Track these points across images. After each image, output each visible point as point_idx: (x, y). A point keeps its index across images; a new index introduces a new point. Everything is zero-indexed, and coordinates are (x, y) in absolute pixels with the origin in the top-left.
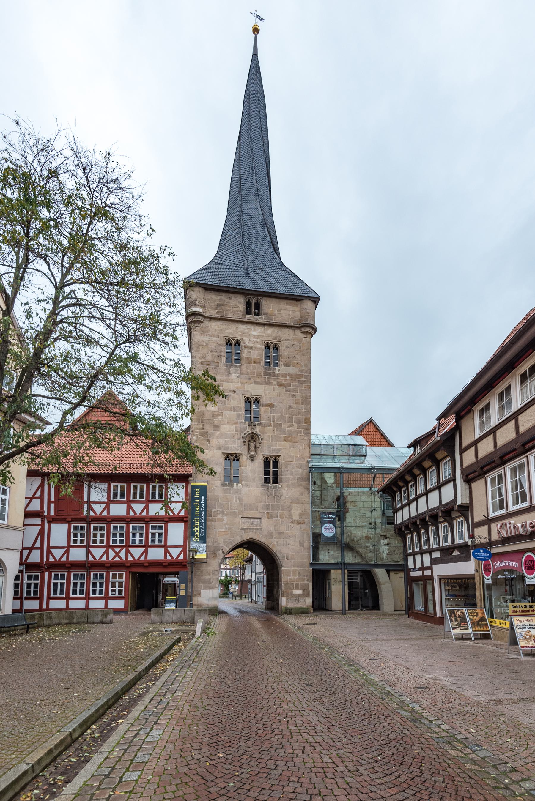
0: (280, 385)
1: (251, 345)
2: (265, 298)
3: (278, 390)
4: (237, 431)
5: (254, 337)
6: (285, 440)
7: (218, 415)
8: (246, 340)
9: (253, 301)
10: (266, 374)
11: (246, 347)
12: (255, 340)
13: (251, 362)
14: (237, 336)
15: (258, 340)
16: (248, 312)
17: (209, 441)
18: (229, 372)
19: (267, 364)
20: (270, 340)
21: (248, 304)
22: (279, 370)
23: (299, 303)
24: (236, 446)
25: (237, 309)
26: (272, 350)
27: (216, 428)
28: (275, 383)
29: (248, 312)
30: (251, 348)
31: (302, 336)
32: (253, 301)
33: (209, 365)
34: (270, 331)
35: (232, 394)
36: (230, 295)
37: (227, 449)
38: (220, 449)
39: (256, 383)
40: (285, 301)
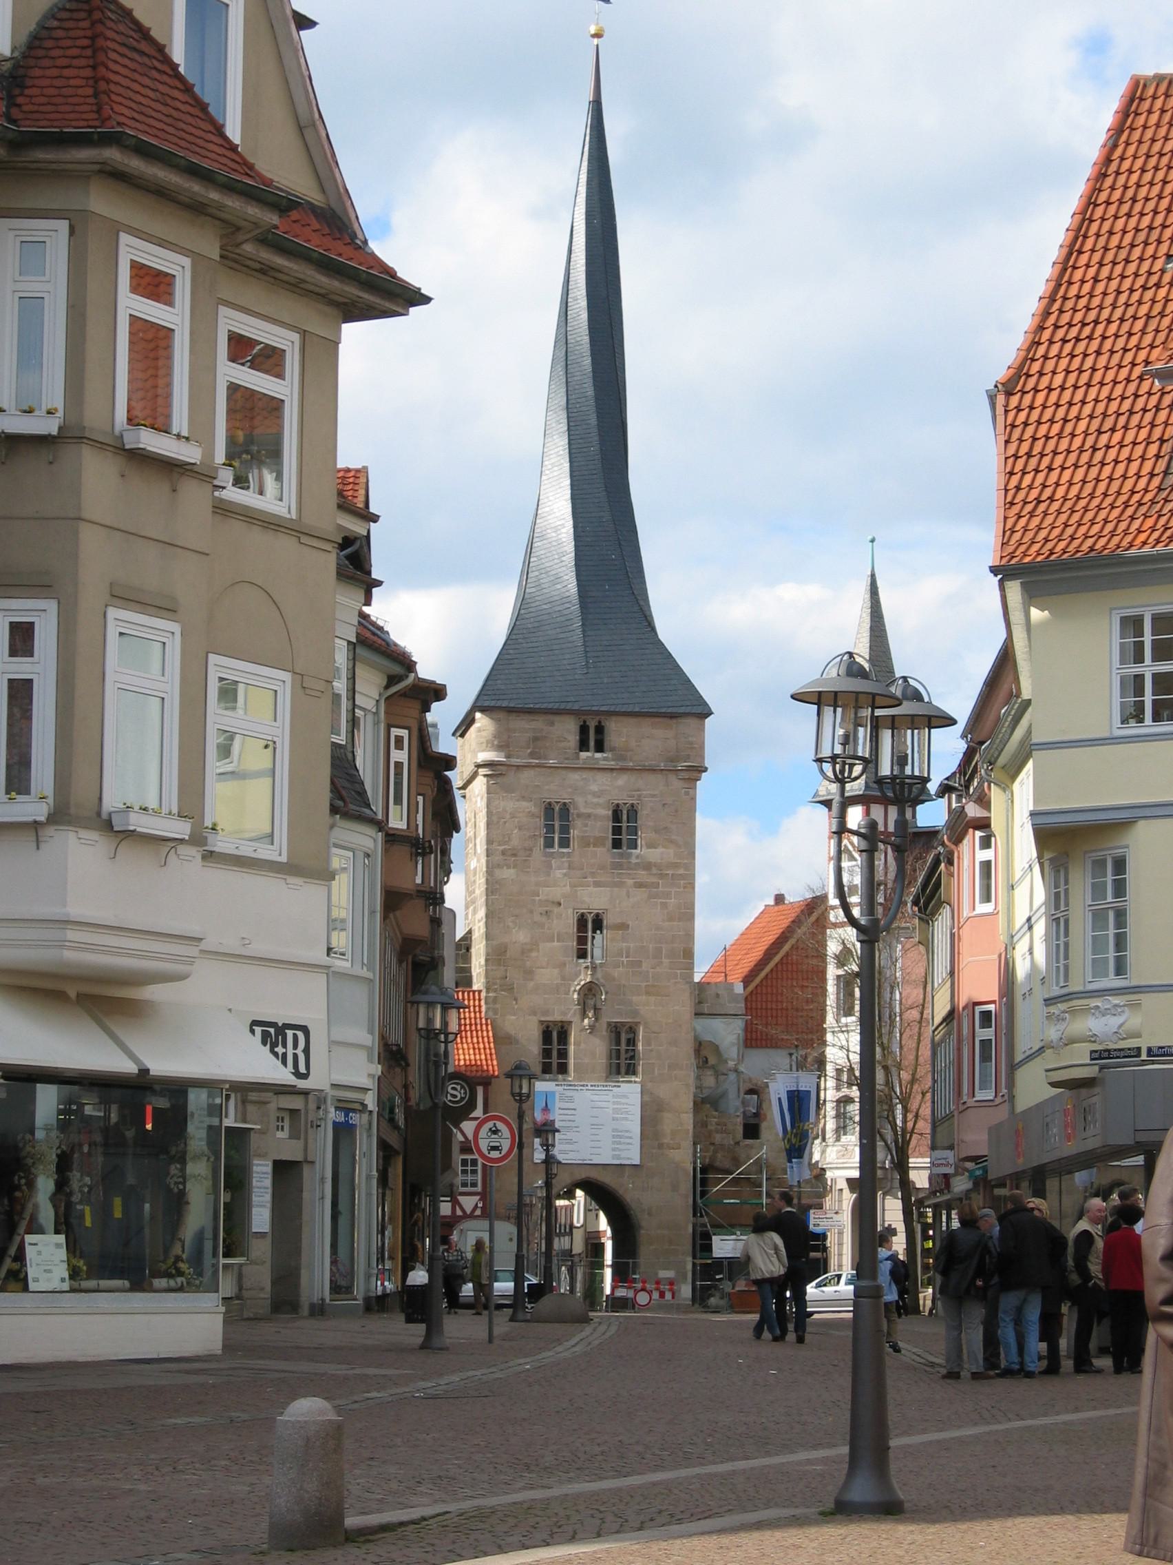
0: (640, 885)
1: (589, 811)
2: (614, 718)
3: (641, 894)
4: (563, 978)
5: (595, 794)
6: (648, 993)
7: (531, 950)
8: (580, 800)
9: (592, 725)
10: (618, 866)
11: (579, 815)
12: (595, 800)
13: (588, 845)
14: (565, 797)
15: (601, 801)
16: (583, 745)
17: (516, 999)
18: (551, 867)
19: (617, 844)
20: (624, 799)
21: (584, 730)
22: (637, 857)
23: (674, 721)
24: (566, 1008)
25: (563, 744)
26: (625, 817)
27: (529, 973)
28: (630, 882)
29: (583, 745)
30: (589, 816)
31: (680, 784)
32: (592, 725)
33: (514, 855)
34: (622, 780)
35: (556, 910)
36: (551, 717)
37: (546, 1012)
38: (534, 1013)
39: (597, 884)
40: (648, 721)
